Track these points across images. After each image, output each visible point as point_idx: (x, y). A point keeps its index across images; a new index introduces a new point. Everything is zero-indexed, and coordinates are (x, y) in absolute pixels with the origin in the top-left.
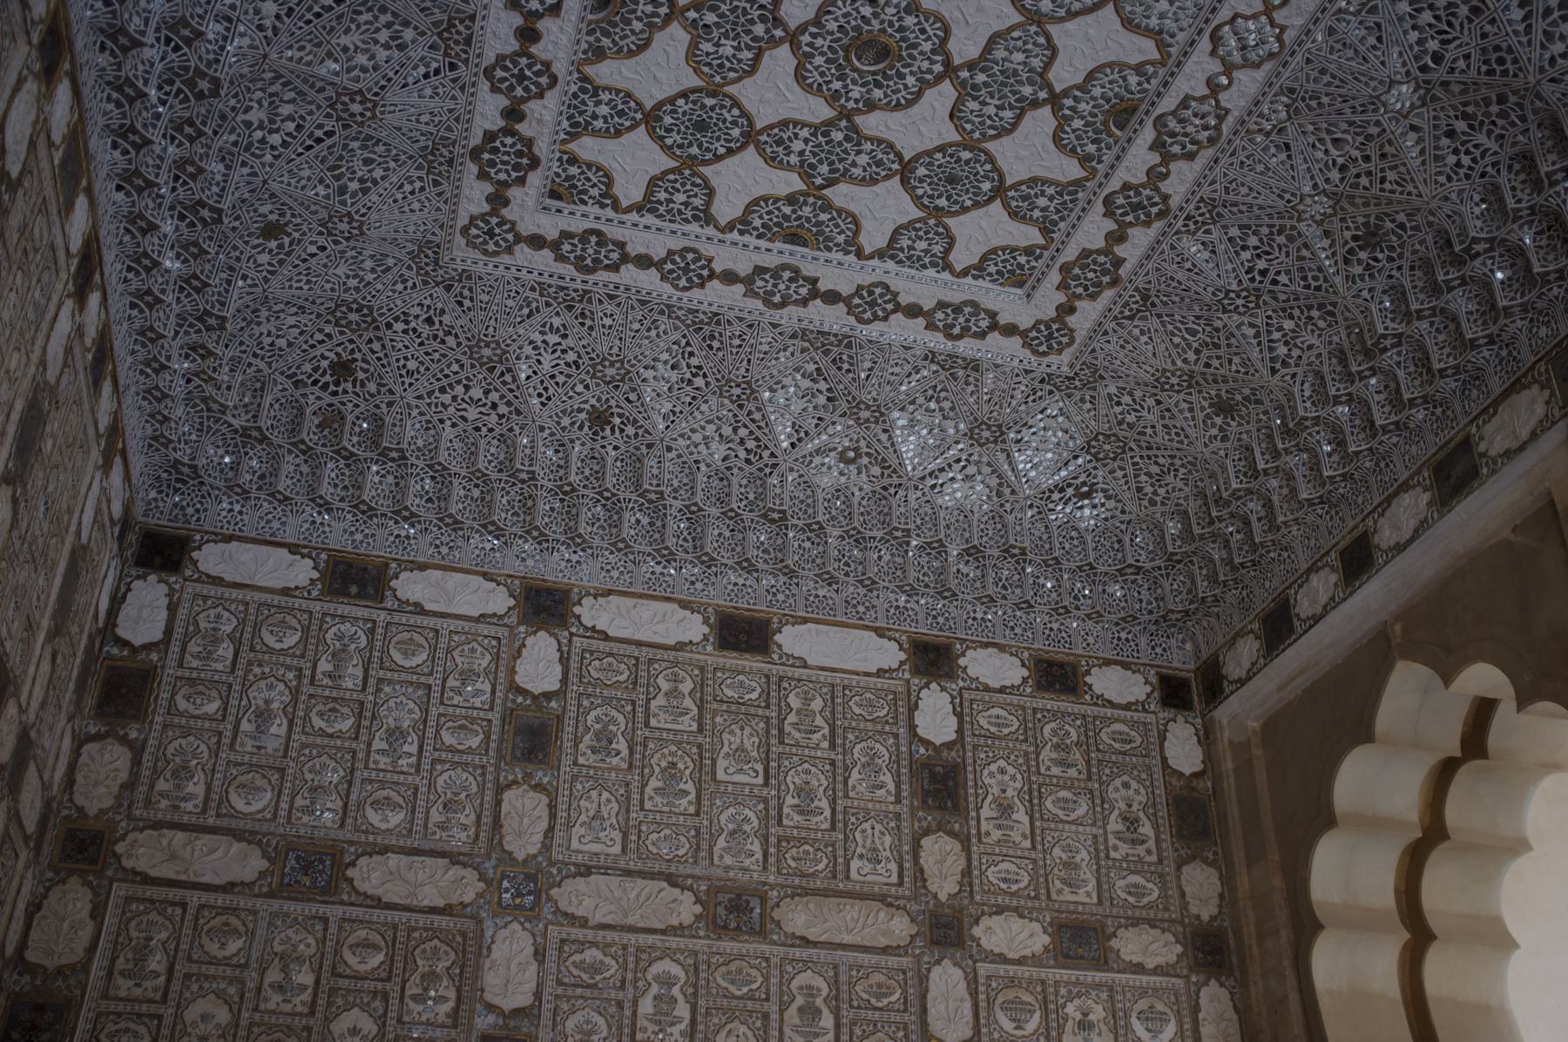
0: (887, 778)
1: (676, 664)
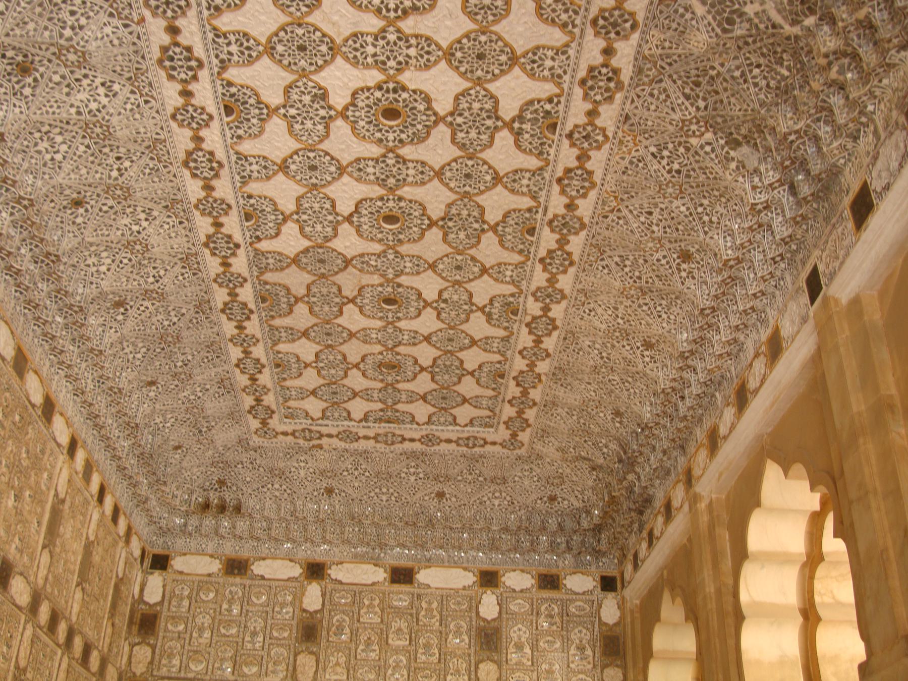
1: (372, 592)
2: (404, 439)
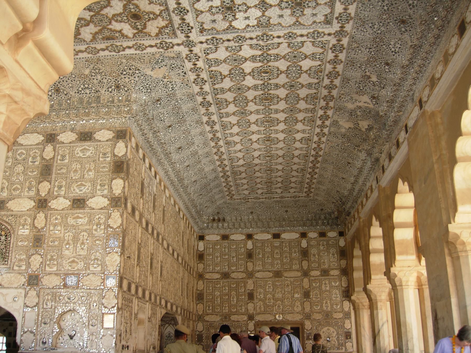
0: (298, 254)
2: (274, 198)
